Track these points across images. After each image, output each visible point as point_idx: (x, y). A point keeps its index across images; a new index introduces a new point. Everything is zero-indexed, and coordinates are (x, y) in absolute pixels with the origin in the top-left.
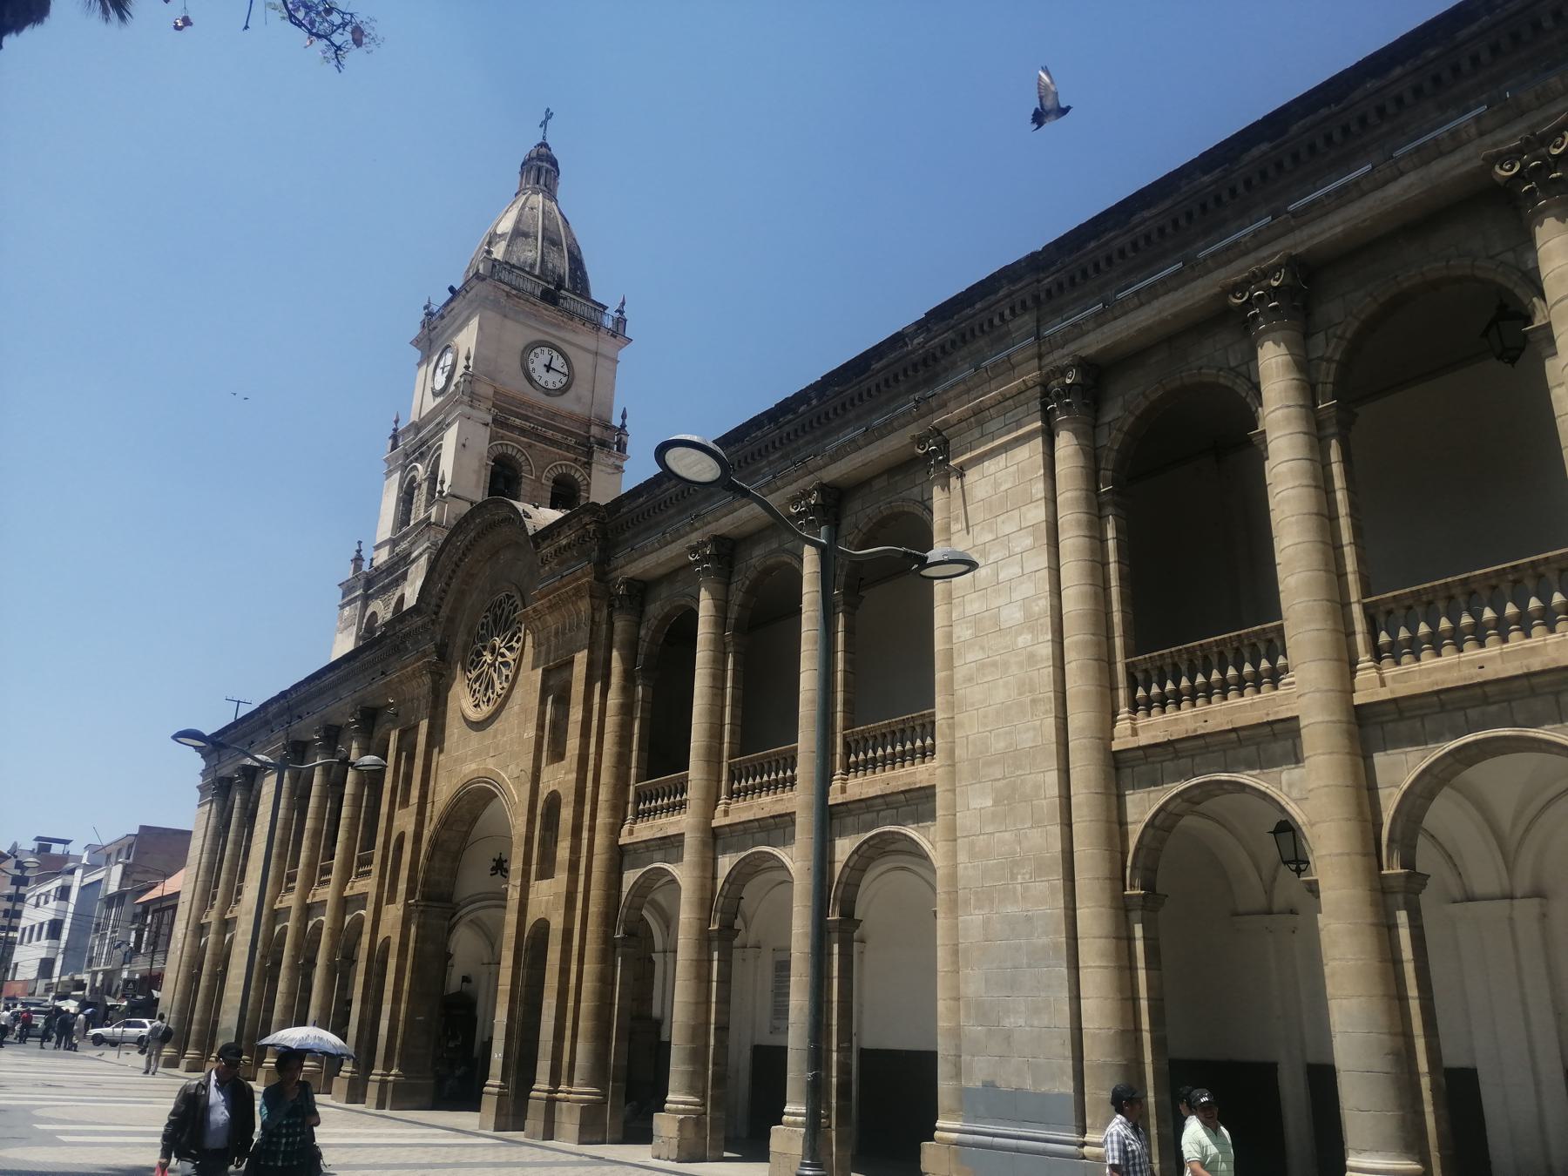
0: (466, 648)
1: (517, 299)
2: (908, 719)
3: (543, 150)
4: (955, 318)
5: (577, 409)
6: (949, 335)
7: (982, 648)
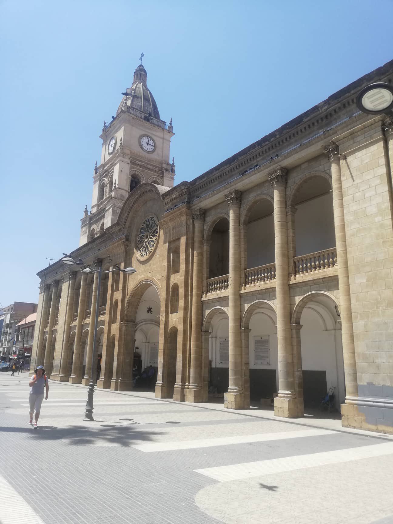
0: (136, 236)
1: (136, 120)
2: (322, 252)
3: (142, 67)
4: (342, 97)
5: (158, 158)
6: (339, 105)
7: (359, 223)
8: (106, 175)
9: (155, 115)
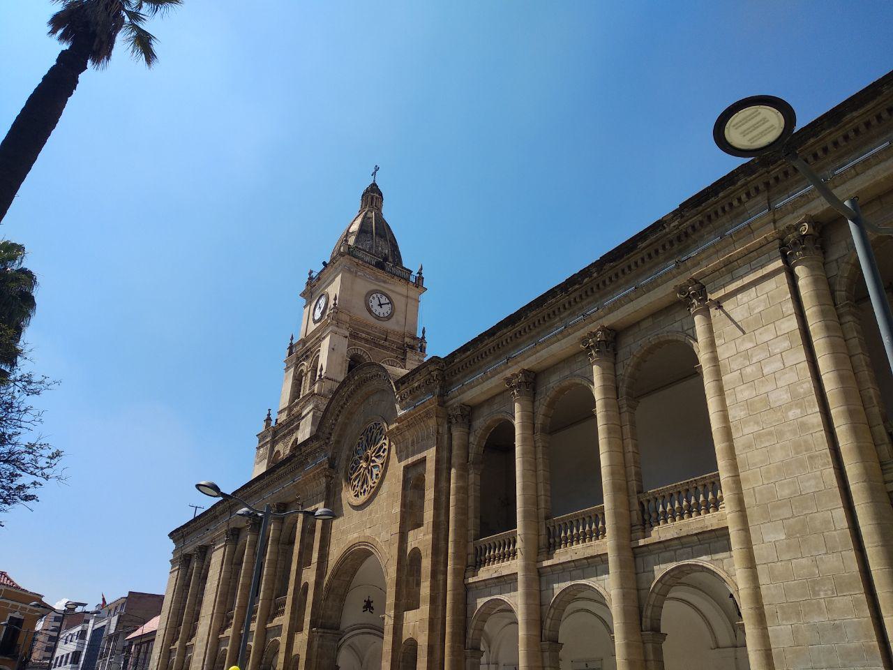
0: (348, 460)
2: (692, 481)
4: (703, 205)
5: (397, 328)
6: (699, 217)
7: (757, 423)
8: (307, 357)
9: (394, 261)
